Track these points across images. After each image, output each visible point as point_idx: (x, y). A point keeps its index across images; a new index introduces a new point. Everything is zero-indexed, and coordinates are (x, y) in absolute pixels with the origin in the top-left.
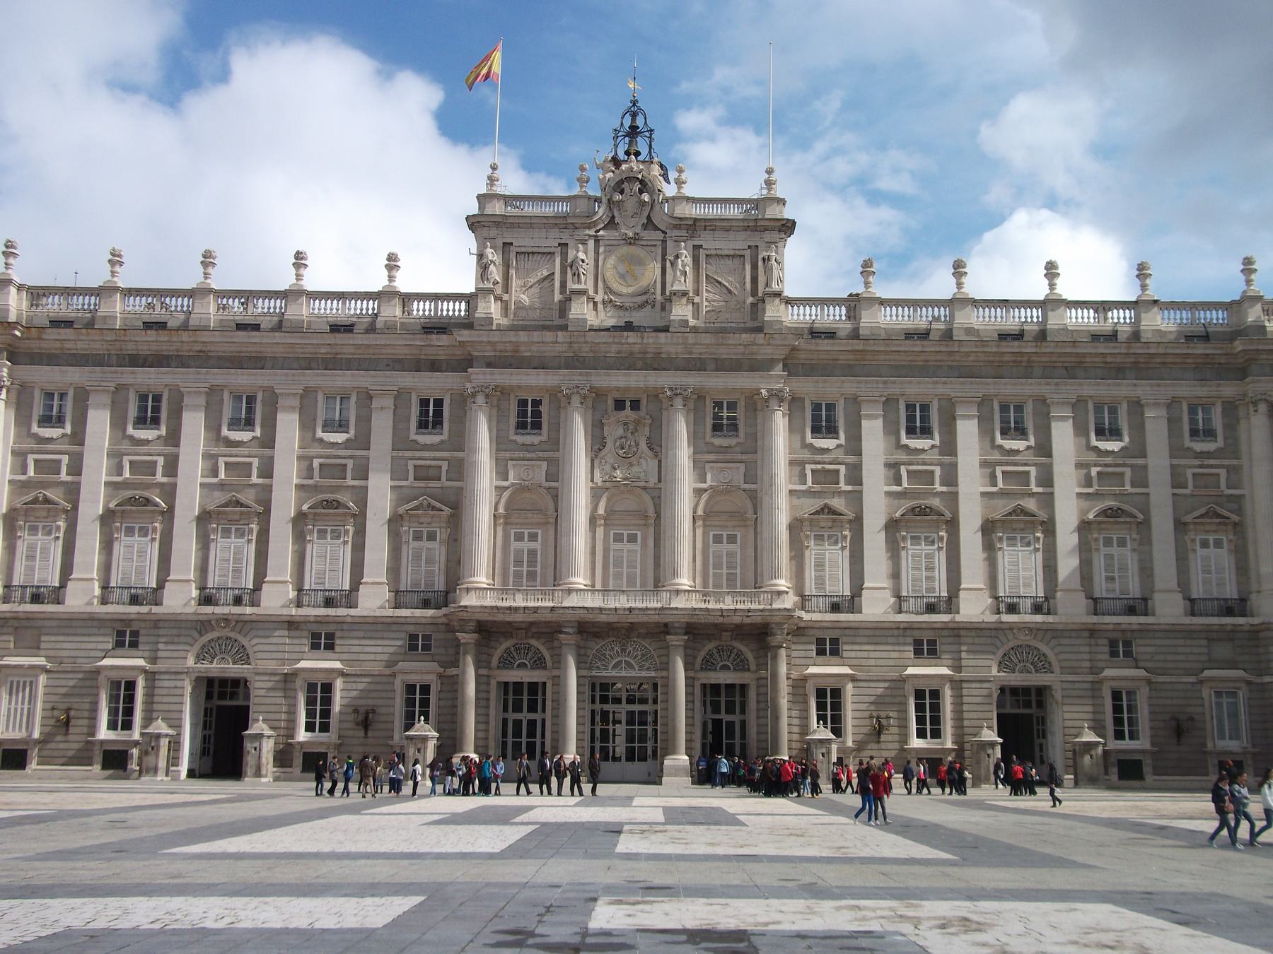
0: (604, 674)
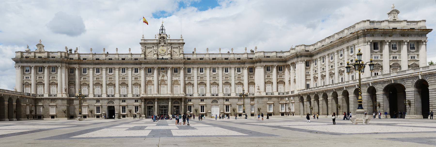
0: (161, 105)
